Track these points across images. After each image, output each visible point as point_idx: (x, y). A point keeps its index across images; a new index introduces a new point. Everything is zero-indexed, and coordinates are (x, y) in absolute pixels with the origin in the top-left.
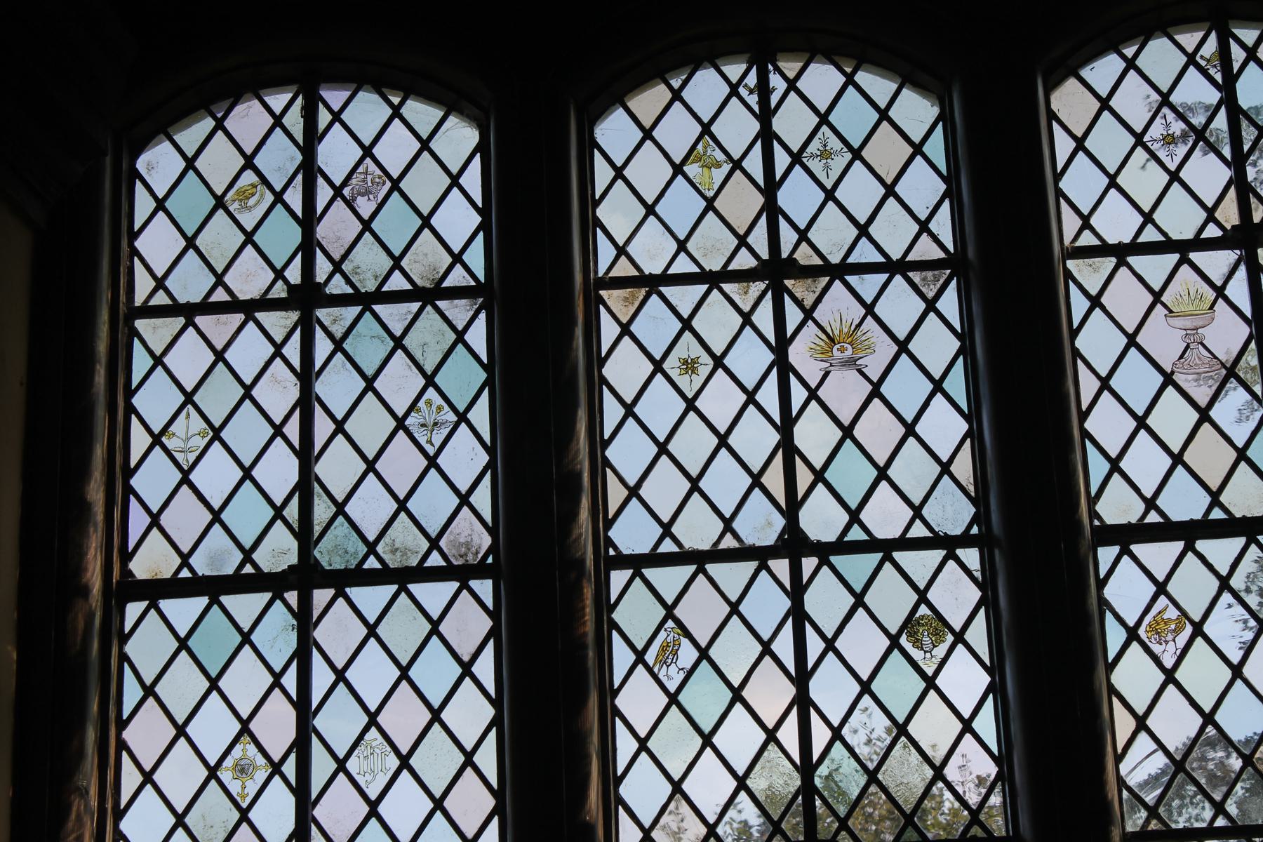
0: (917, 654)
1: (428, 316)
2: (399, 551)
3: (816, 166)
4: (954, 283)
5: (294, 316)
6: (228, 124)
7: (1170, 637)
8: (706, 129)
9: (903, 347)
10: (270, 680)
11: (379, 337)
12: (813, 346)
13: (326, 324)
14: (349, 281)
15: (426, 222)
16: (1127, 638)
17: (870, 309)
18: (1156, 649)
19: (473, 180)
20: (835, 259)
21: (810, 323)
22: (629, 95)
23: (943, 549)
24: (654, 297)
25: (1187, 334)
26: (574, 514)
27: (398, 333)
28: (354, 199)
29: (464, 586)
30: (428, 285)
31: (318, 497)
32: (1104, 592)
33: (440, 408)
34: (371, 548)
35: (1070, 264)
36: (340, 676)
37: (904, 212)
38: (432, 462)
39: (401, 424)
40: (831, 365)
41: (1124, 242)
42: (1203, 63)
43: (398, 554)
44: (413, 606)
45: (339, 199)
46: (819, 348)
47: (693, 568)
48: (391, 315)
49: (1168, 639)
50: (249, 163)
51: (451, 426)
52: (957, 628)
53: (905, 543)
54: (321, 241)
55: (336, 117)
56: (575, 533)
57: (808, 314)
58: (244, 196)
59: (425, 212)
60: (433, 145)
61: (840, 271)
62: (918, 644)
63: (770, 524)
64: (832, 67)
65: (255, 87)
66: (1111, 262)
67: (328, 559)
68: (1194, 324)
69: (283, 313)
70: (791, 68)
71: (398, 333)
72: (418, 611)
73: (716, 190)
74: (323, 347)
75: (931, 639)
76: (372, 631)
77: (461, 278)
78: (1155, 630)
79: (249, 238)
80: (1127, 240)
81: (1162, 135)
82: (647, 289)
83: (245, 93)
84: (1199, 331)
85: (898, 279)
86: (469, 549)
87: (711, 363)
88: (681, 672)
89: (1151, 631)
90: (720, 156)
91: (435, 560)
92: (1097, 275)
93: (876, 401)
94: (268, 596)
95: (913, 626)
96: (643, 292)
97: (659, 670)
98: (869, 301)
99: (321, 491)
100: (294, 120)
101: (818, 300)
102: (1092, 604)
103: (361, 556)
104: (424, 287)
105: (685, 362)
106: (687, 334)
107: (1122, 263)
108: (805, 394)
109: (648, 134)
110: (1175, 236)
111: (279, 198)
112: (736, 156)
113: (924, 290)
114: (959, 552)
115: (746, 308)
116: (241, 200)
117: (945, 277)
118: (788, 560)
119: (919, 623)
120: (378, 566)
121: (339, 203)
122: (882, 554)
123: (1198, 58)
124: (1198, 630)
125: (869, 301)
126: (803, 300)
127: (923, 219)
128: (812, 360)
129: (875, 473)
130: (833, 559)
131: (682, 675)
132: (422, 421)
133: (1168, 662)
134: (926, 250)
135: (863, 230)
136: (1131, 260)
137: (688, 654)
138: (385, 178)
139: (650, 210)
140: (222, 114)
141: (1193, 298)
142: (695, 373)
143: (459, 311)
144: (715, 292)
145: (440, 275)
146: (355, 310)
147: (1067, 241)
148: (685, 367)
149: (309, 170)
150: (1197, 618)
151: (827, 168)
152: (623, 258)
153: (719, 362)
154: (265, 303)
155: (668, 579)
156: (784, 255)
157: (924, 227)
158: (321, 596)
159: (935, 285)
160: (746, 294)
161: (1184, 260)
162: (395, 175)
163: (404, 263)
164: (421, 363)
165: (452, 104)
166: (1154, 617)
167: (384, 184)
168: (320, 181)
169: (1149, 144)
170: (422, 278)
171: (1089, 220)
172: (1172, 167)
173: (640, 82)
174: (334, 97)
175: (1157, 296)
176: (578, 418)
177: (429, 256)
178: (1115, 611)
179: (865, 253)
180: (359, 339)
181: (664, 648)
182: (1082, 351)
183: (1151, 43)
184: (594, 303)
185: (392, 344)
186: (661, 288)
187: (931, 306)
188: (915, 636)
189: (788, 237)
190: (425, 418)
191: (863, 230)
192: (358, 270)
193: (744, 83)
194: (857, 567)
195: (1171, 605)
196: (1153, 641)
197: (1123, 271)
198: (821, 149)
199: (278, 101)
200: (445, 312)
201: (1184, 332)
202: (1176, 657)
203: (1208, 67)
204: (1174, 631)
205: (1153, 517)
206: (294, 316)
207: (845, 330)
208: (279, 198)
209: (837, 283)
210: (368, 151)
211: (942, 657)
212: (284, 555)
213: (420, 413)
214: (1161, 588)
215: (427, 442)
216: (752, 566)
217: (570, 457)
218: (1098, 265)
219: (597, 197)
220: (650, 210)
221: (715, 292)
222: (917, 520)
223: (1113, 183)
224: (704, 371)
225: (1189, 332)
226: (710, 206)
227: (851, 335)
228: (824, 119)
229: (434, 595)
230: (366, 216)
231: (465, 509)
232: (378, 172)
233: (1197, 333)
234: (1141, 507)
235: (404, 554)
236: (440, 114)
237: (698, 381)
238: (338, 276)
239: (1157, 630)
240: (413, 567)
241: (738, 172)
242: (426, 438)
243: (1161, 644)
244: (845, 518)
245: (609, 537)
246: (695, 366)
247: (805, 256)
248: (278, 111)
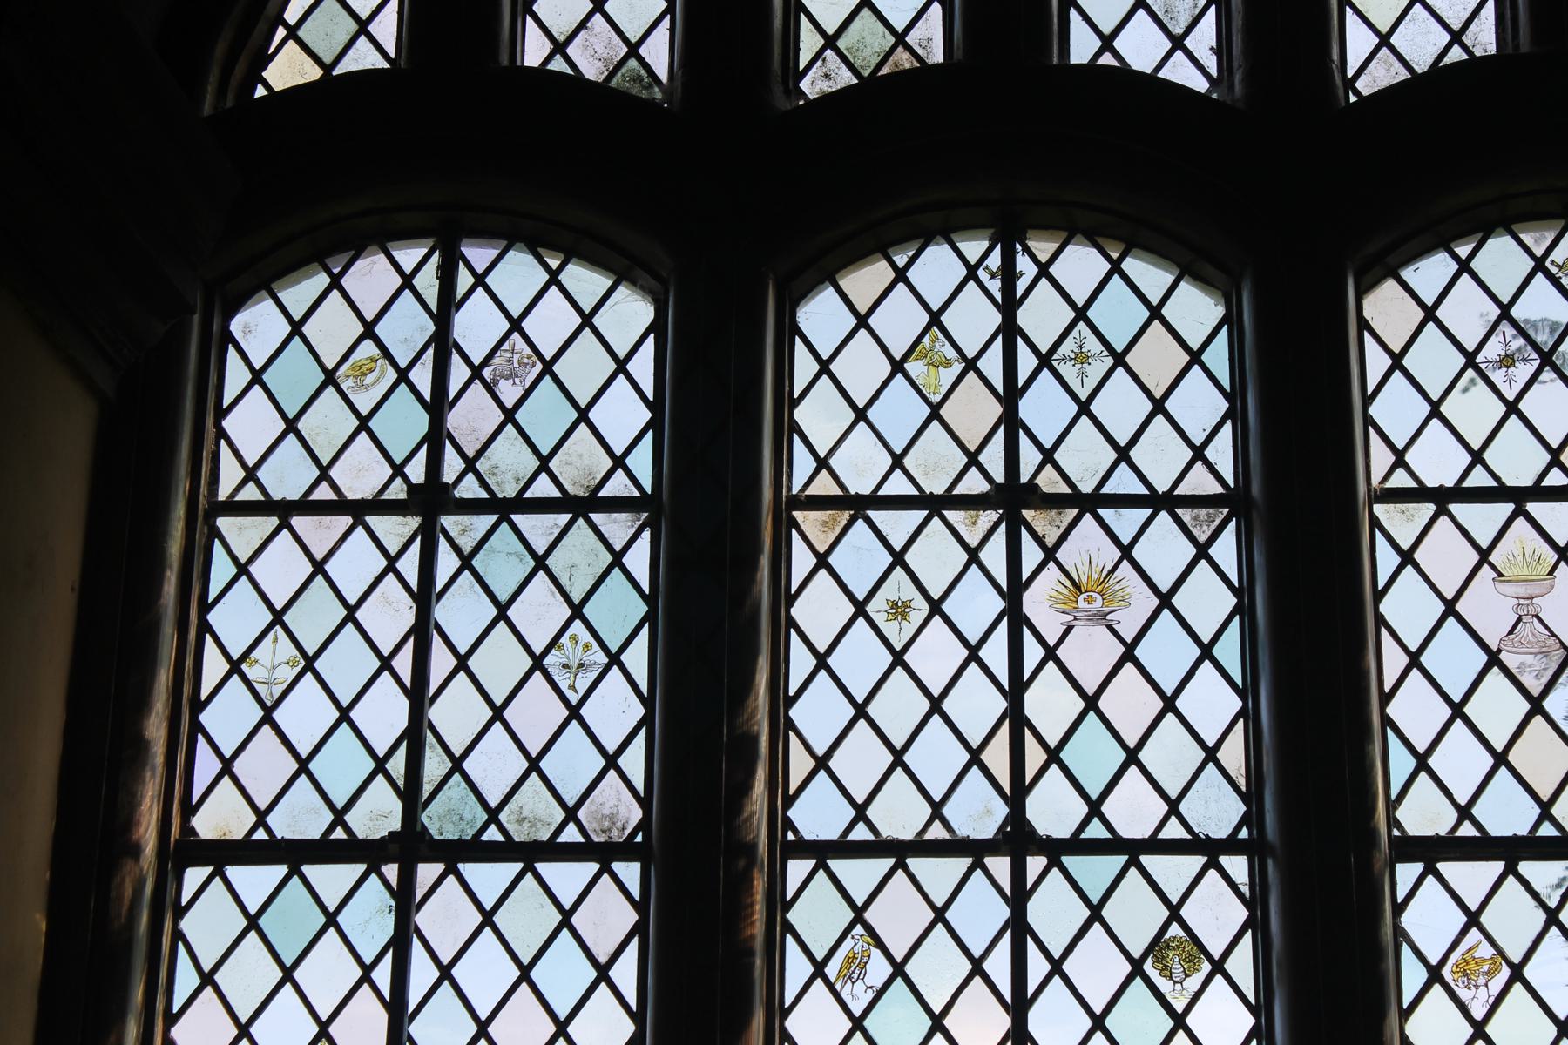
0: (1164, 985)
1: (578, 531)
2: (527, 821)
3: (1068, 371)
4: (1233, 524)
5: (414, 522)
6: (345, 282)
7: (1481, 981)
8: (935, 319)
9: (1165, 600)
10: (358, 973)
11: (517, 554)
12: (1055, 594)
13: (453, 534)
14: (483, 483)
15: (583, 415)
16: (1427, 979)
17: (1126, 552)
18: (1463, 994)
19: (643, 367)
20: (1086, 487)
21: (1051, 564)
22: (842, 272)
23: (1203, 855)
24: (860, 523)
25: (1519, 604)
26: (746, 787)
27: (541, 551)
28: (496, 383)
29: (606, 869)
30: (581, 493)
31: (430, 748)
32: (1402, 919)
33: (587, 647)
34: (493, 815)
35: (1379, 509)
36: (445, 973)
37: (1175, 434)
38: (574, 713)
39: (538, 663)
40: (1075, 619)
41: (1446, 485)
42: (1554, 270)
43: (526, 825)
44: (541, 891)
45: (477, 381)
46: (1061, 597)
47: (891, 862)
48: (533, 528)
49: (1479, 983)
50: (369, 331)
51: (600, 670)
52: (1216, 955)
53: (1155, 845)
54: (452, 432)
55: (480, 280)
56: (748, 810)
57: (1050, 554)
58: (361, 372)
59: (583, 404)
60: (596, 321)
61: (1091, 503)
62: (1166, 972)
63: (989, 812)
64: (1095, 250)
65: (382, 238)
66: (1429, 509)
67: (438, 827)
68: (1529, 592)
69: (400, 519)
70: (1043, 249)
71: (541, 551)
72: (546, 896)
73: (943, 394)
74: (447, 562)
75: (1183, 966)
76: (488, 918)
77: (622, 487)
78: (1464, 971)
79: (364, 424)
80: (1450, 483)
81: (1500, 355)
82: (852, 512)
83: (370, 245)
84: (1535, 601)
85: (1164, 516)
86: (614, 823)
87: (926, 608)
88: (869, 990)
89: (1458, 972)
90: (950, 353)
91: (571, 835)
92: (1410, 523)
93: (1129, 666)
94: (361, 868)
95: (1161, 949)
96: (846, 515)
97: (842, 987)
98: (1126, 541)
99: (434, 741)
100: (428, 282)
101: (1063, 537)
102: (1386, 934)
103: (479, 825)
104: (576, 495)
105: (894, 605)
106: (899, 571)
107: (1442, 511)
108: (1041, 653)
109: (862, 321)
110: (1510, 481)
111: (403, 376)
112: (970, 354)
113: (1194, 531)
114: (1223, 860)
115: (973, 542)
116: (356, 377)
117: (1222, 517)
118: (1009, 858)
119: (1168, 946)
120: (500, 838)
121: (477, 386)
122: (1127, 857)
123: (1548, 264)
124: (1517, 974)
125: (1126, 542)
126: (1044, 536)
127: (1198, 444)
128: (1051, 611)
129: (1123, 755)
130: (1065, 860)
131: (870, 995)
132: (565, 661)
133: (1478, 1013)
134: (1200, 482)
135: (1123, 454)
136: (1454, 508)
137: (879, 969)
138: (535, 358)
139: (861, 415)
140: (339, 269)
141: (1529, 560)
142: (905, 619)
143: (618, 527)
144: (936, 520)
145: (597, 481)
146: (491, 519)
147: (1375, 481)
148: (894, 611)
149: (443, 344)
150: (1516, 959)
151: (1082, 375)
152: (824, 472)
153: (936, 607)
154: (378, 505)
155: (860, 874)
156: (1024, 479)
157: (1199, 453)
158: (427, 872)
159: (1209, 526)
160: (974, 524)
161: (1519, 512)
162: (548, 356)
163: (553, 465)
164: (568, 589)
165: (623, 271)
166: (1463, 955)
167: (533, 366)
168: (456, 357)
169: (1483, 366)
170: (574, 485)
171: (1404, 456)
172: (1511, 397)
173: (856, 257)
174: (478, 254)
175: (1484, 555)
176: (759, 667)
177: (585, 457)
178: (1415, 945)
179: (1124, 483)
180: (493, 555)
181: (849, 960)
182: (1387, 618)
183: (1490, 242)
184: (785, 526)
185: (532, 563)
186: (869, 512)
187: (1202, 552)
188: (1164, 962)
189: (1029, 457)
190: (568, 658)
191: (1123, 454)
192: (496, 471)
193: (984, 265)
194: (1095, 871)
195: (1484, 941)
196: (1460, 984)
197: (1444, 521)
198: (1077, 350)
199: (409, 256)
200: (600, 527)
201: (1516, 601)
202: (1488, 1007)
203: (1560, 275)
204: (1487, 973)
205: (1467, 830)
206: (414, 522)
207: (1095, 576)
208: (403, 376)
209: (1088, 516)
210: (516, 325)
211: (1196, 990)
212: (383, 818)
213: (563, 652)
214: (1473, 919)
215: (570, 687)
216: (964, 863)
217: (746, 716)
218: (1412, 511)
219: (796, 396)
220: (861, 415)
221: (936, 520)
222: (1173, 817)
223: (1435, 412)
224: (917, 618)
225: (1522, 601)
226: (935, 413)
227: (1102, 583)
228: (1081, 314)
229: (567, 877)
230: (509, 404)
231: (612, 772)
232: (528, 351)
233: (1532, 604)
234: (1453, 815)
235: (533, 825)
237: (909, 629)
238: (470, 476)
239: (1465, 970)
240: (542, 843)
241: (971, 374)
242: (568, 682)
243: (1469, 988)
244: (1084, 809)
245: (789, 817)
246: (907, 610)
247: (1049, 482)
248: (408, 270)
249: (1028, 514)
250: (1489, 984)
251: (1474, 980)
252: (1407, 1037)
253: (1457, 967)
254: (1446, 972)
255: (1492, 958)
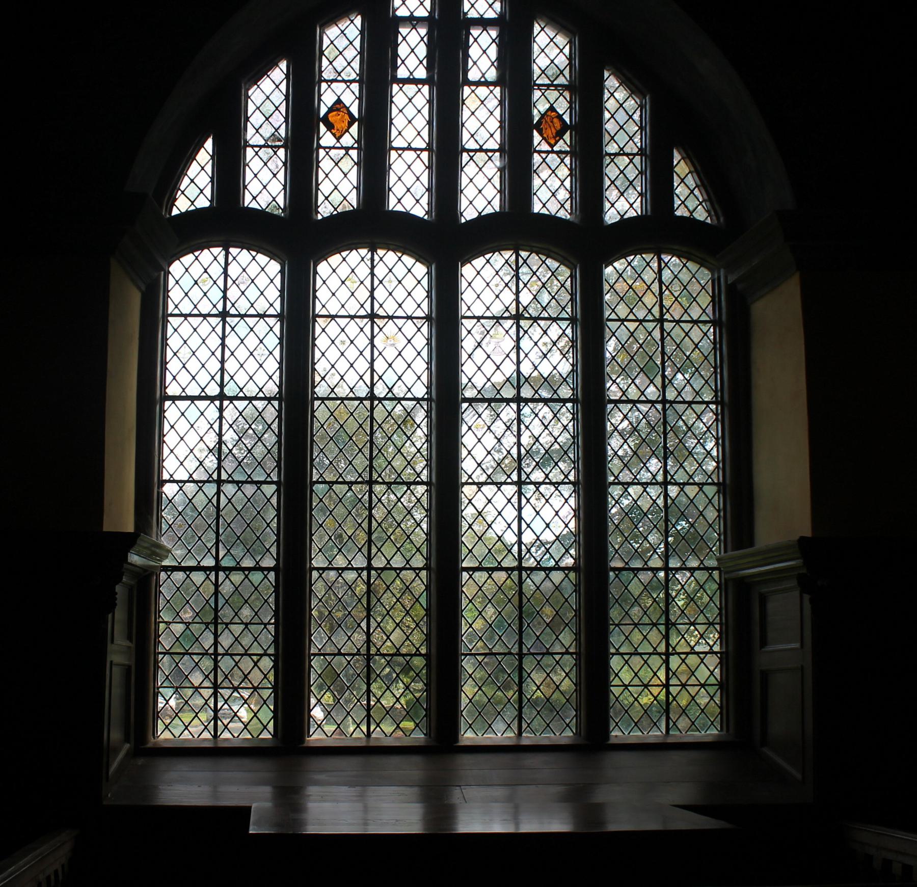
8: (353, 271)
17: (400, 329)
20: (390, 315)
30: (263, 313)
33: (264, 350)
42: (510, 263)
62: (406, 427)
74: (228, 329)
80: (481, 315)
87: (350, 342)
90: (357, 279)
107: (478, 321)
108: (378, 353)
134: (419, 313)
143: (272, 321)
151: (390, 285)
153: (352, 342)
160: (362, 322)
165: (272, 256)
179: (400, 313)
181: (330, 424)
220: (334, 294)
236: (269, 259)
249: (375, 320)
254: (472, 428)
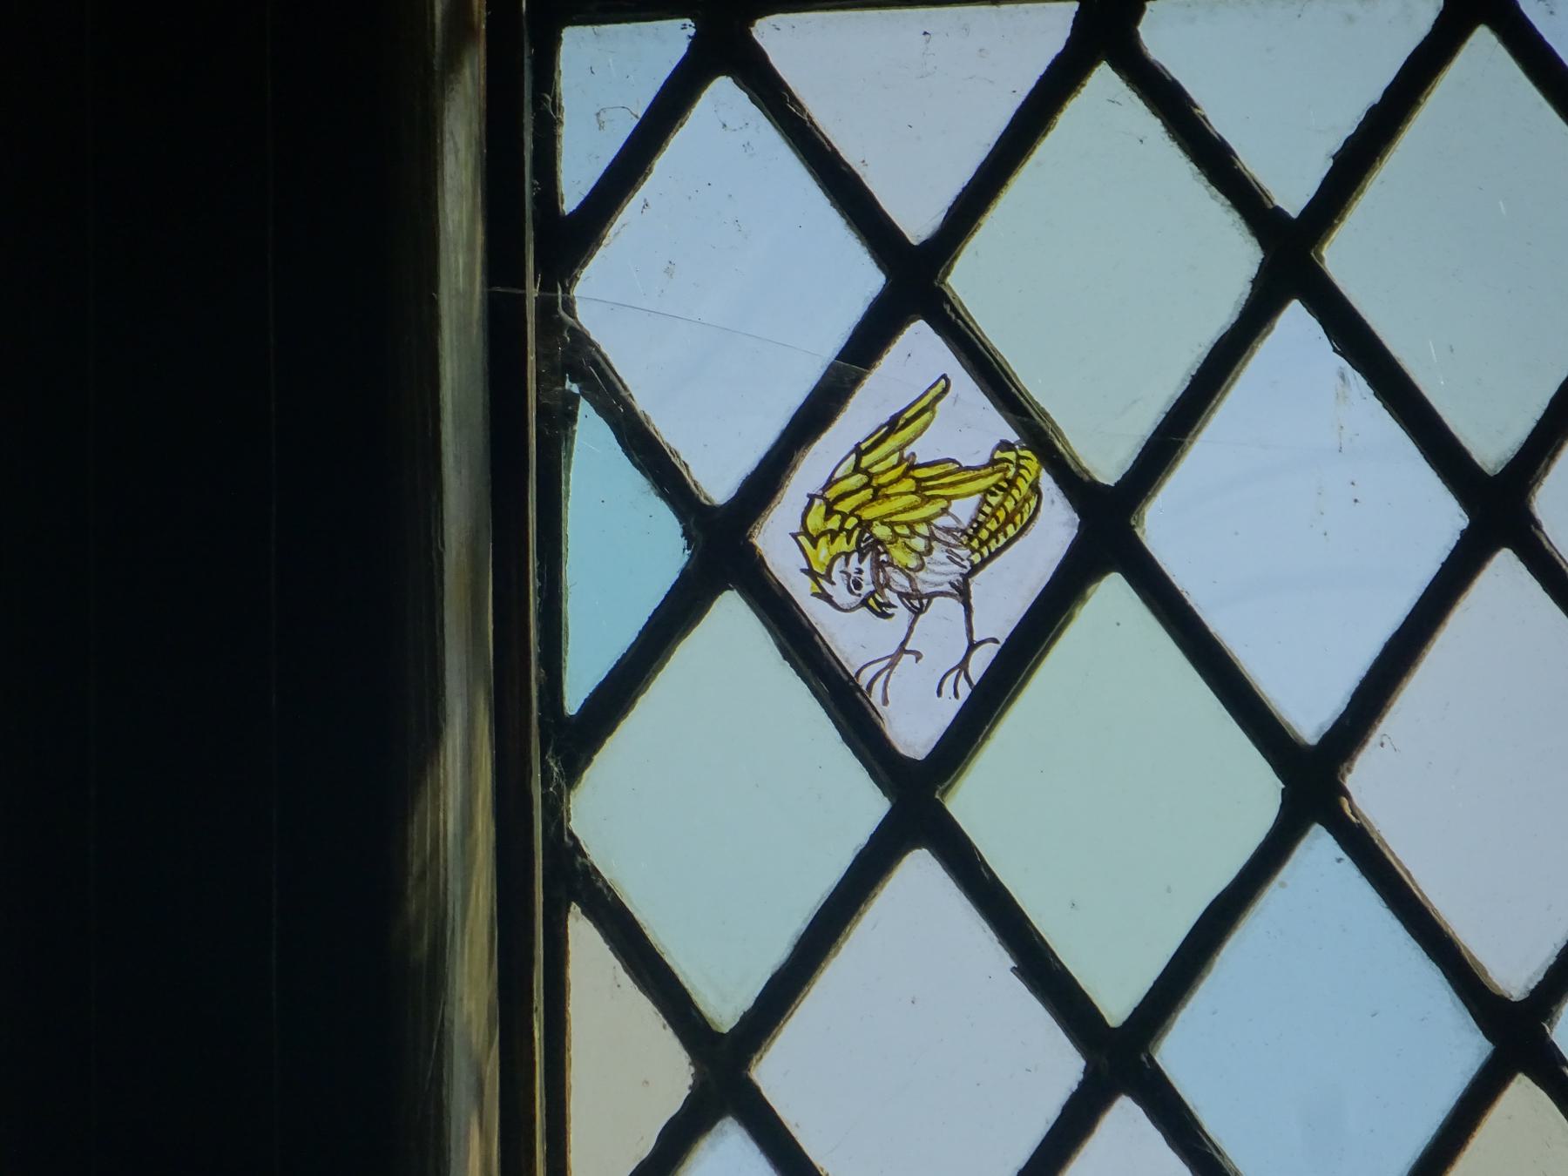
16: (685, 575)
32: (578, 291)
49: (928, 580)
89: (833, 534)
166: (859, 452)
178: (630, 409)
196: (839, 592)
202: (965, 691)
239: (865, 525)
243: (882, 611)
250: (976, 585)
251: (904, 570)
252: (577, 849)
253: (830, 513)
255: (993, 462)
